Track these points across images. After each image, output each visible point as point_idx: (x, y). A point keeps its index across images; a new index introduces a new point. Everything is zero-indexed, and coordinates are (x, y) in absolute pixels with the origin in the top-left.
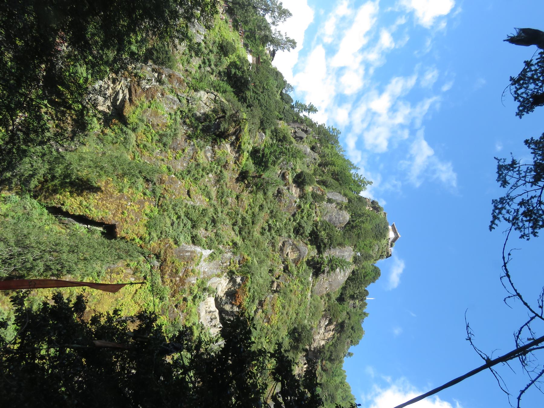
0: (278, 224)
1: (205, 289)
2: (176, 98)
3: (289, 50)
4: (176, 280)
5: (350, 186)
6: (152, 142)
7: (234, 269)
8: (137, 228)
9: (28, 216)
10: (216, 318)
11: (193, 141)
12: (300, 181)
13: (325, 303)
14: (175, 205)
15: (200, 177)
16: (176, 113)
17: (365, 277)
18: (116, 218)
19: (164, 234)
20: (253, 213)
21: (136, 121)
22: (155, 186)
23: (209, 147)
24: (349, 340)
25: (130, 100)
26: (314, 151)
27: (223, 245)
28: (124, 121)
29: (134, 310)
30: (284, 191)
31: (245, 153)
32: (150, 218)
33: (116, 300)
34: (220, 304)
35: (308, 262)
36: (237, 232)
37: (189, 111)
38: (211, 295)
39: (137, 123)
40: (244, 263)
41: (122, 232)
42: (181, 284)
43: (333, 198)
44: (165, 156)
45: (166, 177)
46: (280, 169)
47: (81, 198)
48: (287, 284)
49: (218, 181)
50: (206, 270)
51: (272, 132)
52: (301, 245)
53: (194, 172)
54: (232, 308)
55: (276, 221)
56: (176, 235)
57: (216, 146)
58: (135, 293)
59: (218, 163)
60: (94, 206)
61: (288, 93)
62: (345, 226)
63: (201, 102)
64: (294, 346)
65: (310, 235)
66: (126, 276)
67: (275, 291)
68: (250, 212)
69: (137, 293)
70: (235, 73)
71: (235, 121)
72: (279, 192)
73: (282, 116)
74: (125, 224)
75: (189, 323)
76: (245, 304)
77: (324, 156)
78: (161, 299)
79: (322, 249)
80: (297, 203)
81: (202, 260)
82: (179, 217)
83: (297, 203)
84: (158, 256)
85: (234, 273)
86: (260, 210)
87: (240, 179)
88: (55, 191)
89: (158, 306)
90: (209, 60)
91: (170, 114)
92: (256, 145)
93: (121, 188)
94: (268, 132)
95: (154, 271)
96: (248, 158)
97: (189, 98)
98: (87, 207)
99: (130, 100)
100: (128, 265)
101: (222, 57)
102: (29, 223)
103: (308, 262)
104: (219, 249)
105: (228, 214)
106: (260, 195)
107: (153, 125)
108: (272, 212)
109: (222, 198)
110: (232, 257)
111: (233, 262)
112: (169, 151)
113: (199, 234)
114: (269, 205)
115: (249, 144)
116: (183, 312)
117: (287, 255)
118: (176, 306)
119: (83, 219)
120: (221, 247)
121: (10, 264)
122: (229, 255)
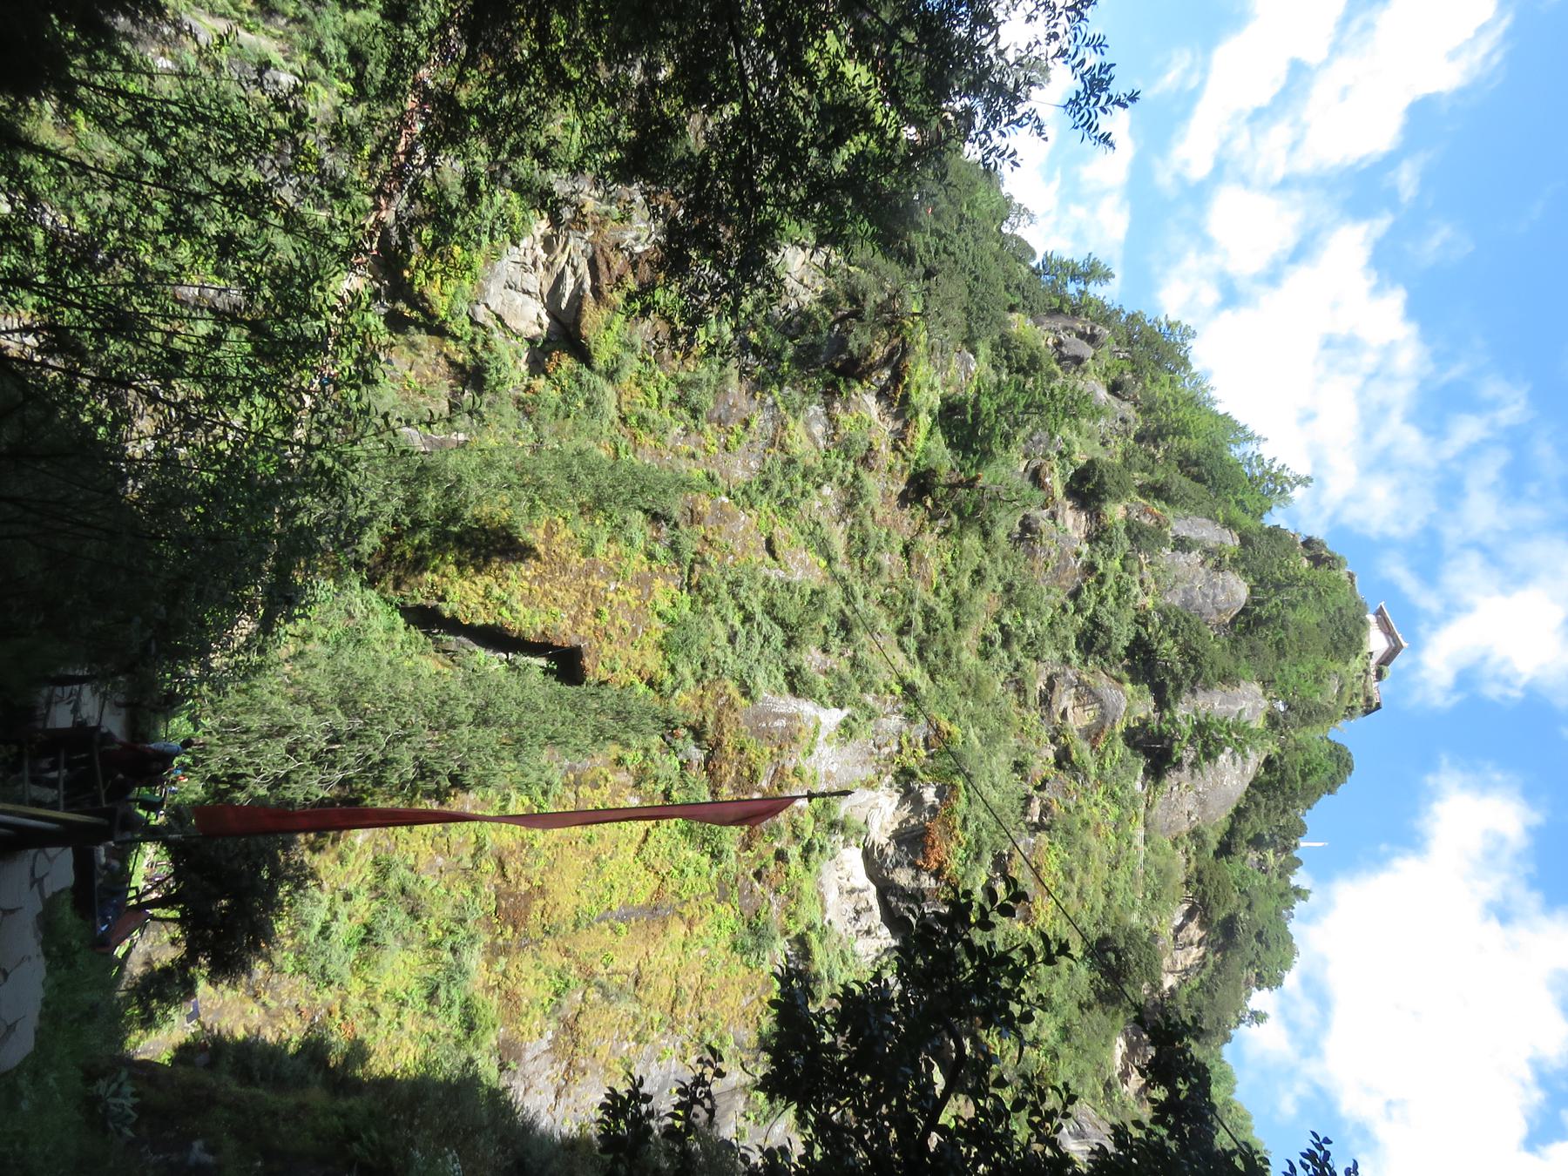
0: (1028, 623)
1: (833, 825)
5: (1239, 497)
6: (660, 407)
7: (912, 763)
8: (637, 653)
10: (871, 909)
11: (770, 394)
12: (1087, 489)
13: (1188, 861)
14: (737, 583)
15: (798, 497)
17: (1304, 776)
18: (582, 630)
19: (711, 667)
20: (955, 594)
21: (616, 349)
22: (677, 533)
23: (820, 410)
24: (1251, 974)
26: (1118, 396)
27: (877, 692)
30: (1042, 524)
32: (672, 623)
33: (596, 860)
34: (881, 868)
35: (1130, 737)
36: (913, 655)
38: (853, 841)
39: (617, 357)
40: (939, 742)
41: (600, 666)
43: (1193, 536)
44: (698, 445)
45: (704, 505)
46: (1026, 456)
47: (487, 579)
48: (1072, 805)
49: (850, 505)
51: (994, 347)
52: (1103, 684)
53: (780, 483)
54: (916, 878)
55: (1023, 615)
57: (837, 405)
58: (645, 840)
59: (847, 451)
60: (517, 598)
61: (1018, 232)
62: (1233, 621)
64: (1107, 992)
65: (1130, 652)
66: (616, 793)
67: (1038, 827)
68: (945, 591)
69: (650, 839)
71: (888, 325)
72: (1027, 526)
73: (1017, 299)
75: (796, 923)
76: (953, 865)
77: (1150, 410)
78: (716, 856)
79: (1169, 695)
80: (1084, 557)
81: (820, 738)
82: (748, 618)
83: (1084, 557)
84: (698, 733)
85: (913, 775)
86: (973, 584)
87: (911, 496)
88: (419, 565)
89: (709, 876)
92: (951, 390)
93: (587, 542)
94: (984, 349)
95: (691, 775)
96: (931, 432)
99: (596, 291)
100: (620, 761)
102: (362, 654)
103: (1130, 737)
104: (865, 706)
106: (972, 541)
108: (1009, 588)
109: (864, 554)
110: (905, 728)
111: (909, 741)
112: (707, 427)
113: (806, 665)
114: (1001, 568)
115: (932, 388)
116: (777, 891)
117: (1064, 715)
118: (758, 875)
119: (495, 638)
120: (869, 698)
122: (895, 721)
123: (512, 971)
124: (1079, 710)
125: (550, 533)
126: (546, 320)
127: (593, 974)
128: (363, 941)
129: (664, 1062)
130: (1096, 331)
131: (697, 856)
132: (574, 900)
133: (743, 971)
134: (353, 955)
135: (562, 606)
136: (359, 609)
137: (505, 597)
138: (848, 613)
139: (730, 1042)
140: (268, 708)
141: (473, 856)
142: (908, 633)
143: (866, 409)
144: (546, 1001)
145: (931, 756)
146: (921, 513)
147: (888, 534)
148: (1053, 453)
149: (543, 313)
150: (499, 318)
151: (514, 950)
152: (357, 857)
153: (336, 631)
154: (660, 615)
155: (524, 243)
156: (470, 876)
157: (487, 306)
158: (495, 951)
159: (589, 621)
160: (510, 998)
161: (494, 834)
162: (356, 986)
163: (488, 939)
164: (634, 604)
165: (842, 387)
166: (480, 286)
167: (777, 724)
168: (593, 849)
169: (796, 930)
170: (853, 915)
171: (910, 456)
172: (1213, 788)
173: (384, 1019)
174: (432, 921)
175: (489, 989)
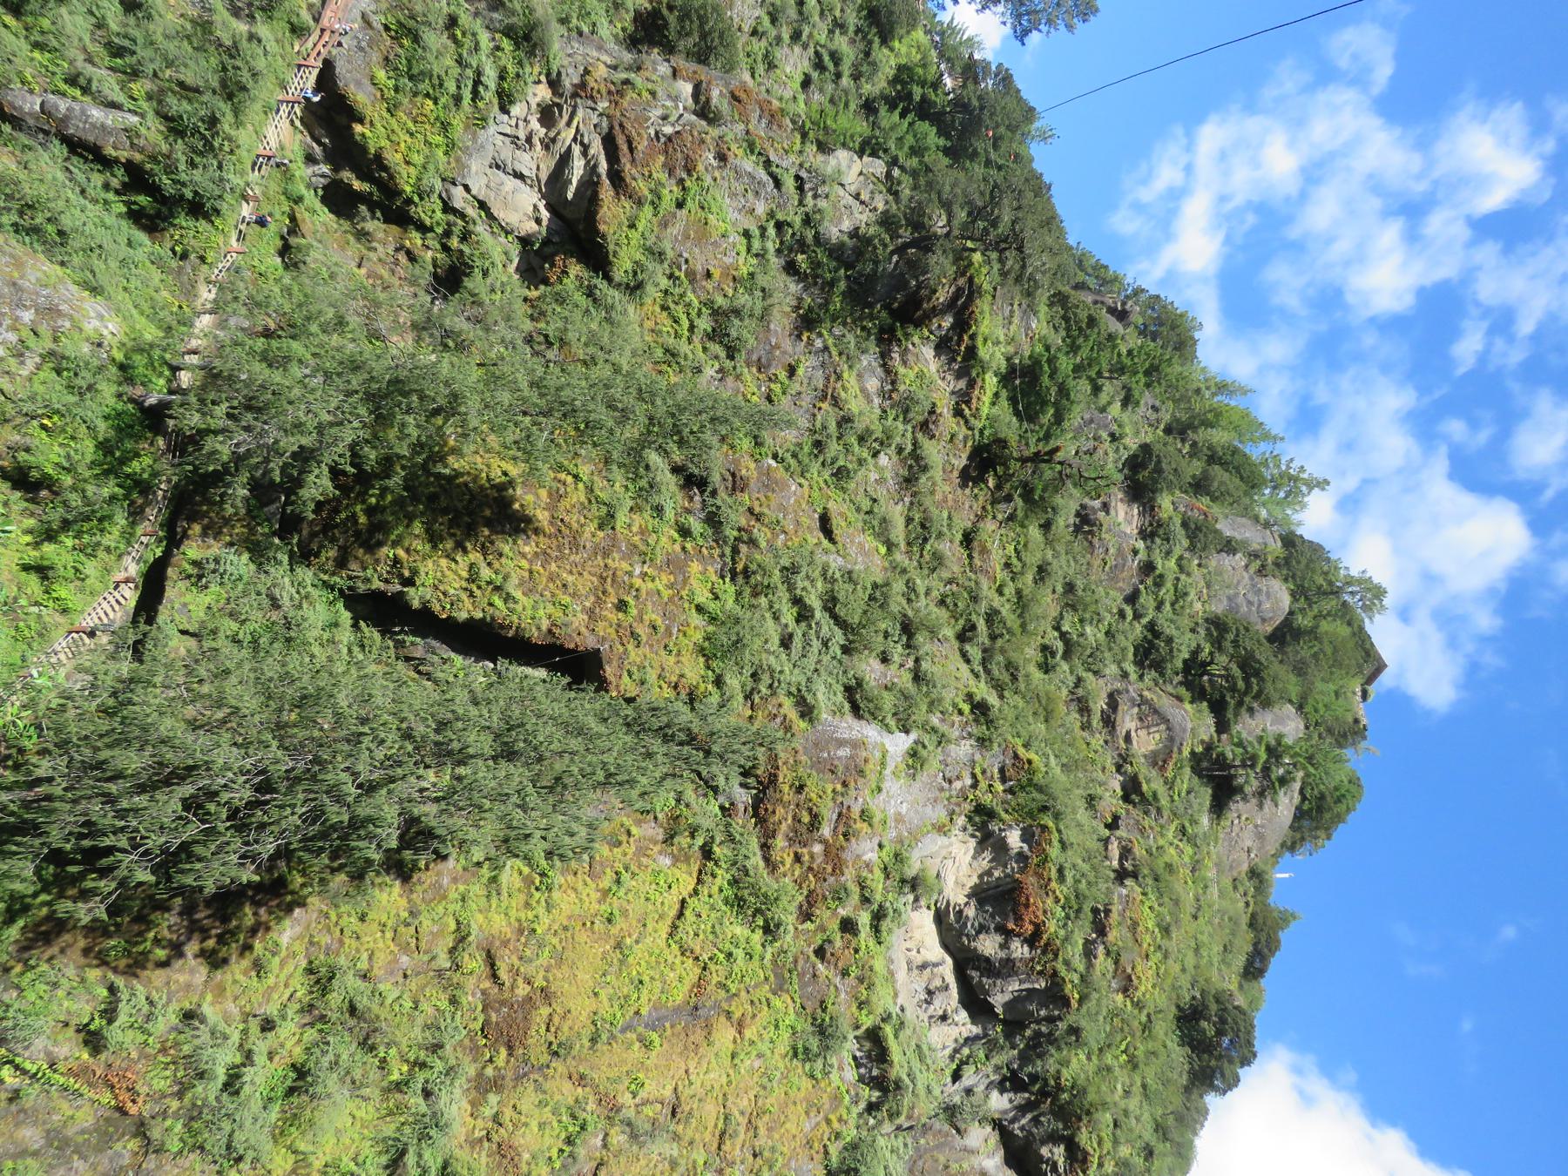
0: (1088, 629)
2: (762, 174)
3: (1070, 27)
4: (812, 856)
7: (987, 799)
8: (672, 659)
9: (288, 634)
10: (947, 988)
11: (820, 335)
13: (1247, 904)
16: (763, 229)
19: (766, 678)
20: (1019, 593)
23: (869, 360)
25: (617, 178)
28: (597, 258)
29: (680, 979)
31: (987, 377)
32: (713, 619)
33: (618, 946)
34: (960, 934)
37: (807, 221)
38: (923, 903)
40: (1019, 777)
42: (829, 869)
43: (1238, 537)
45: (748, 468)
49: (909, 481)
50: (904, 809)
58: (680, 915)
63: (841, 192)
67: (1121, 875)
68: (1009, 590)
69: (688, 913)
70: (923, 96)
74: (630, 647)
78: (770, 930)
79: (1230, 715)
81: (888, 772)
82: (804, 615)
83: (1142, 556)
88: (370, 539)
90: (836, 57)
91: (747, 234)
96: (996, 395)
97: (804, 174)
98: (497, 589)
101: (876, 45)
105: (942, 602)
107: (691, 275)
109: (925, 540)
110: (978, 757)
111: (984, 772)
116: (845, 973)
117: (1128, 738)
119: (484, 640)
120: (935, 720)
121: (262, 826)
122: (963, 750)
123: (508, 1113)
124: (1142, 733)
125: (557, 496)
126: (545, 215)
127: (617, 1109)
128: (291, 1091)
130: (1128, 307)
131: (747, 932)
132: (590, 1004)
133: (806, 1084)
134: (274, 1114)
135: (574, 595)
137: (499, 580)
138: (910, 613)
140: (153, 737)
141: (452, 951)
142: (970, 640)
143: (923, 362)
145: (1010, 791)
146: (983, 495)
147: (950, 518)
148: (1104, 435)
149: (541, 205)
150: (483, 205)
151: (509, 1083)
152: (283, 964)
155: (517, 110)
157: (467, 188)
158: (483, 1086)
159: (614, 616)
161: (480, 918)
163: (471, 1070)
164: (666, 593)
165: (899, 334)
166: (458, 160)
167: (841, 753)
169: (867, 1022)
170: (923, 996)
171: (972, 420)
172: (1270, 820)
174: (393, 1052)
175: (474, 1143)
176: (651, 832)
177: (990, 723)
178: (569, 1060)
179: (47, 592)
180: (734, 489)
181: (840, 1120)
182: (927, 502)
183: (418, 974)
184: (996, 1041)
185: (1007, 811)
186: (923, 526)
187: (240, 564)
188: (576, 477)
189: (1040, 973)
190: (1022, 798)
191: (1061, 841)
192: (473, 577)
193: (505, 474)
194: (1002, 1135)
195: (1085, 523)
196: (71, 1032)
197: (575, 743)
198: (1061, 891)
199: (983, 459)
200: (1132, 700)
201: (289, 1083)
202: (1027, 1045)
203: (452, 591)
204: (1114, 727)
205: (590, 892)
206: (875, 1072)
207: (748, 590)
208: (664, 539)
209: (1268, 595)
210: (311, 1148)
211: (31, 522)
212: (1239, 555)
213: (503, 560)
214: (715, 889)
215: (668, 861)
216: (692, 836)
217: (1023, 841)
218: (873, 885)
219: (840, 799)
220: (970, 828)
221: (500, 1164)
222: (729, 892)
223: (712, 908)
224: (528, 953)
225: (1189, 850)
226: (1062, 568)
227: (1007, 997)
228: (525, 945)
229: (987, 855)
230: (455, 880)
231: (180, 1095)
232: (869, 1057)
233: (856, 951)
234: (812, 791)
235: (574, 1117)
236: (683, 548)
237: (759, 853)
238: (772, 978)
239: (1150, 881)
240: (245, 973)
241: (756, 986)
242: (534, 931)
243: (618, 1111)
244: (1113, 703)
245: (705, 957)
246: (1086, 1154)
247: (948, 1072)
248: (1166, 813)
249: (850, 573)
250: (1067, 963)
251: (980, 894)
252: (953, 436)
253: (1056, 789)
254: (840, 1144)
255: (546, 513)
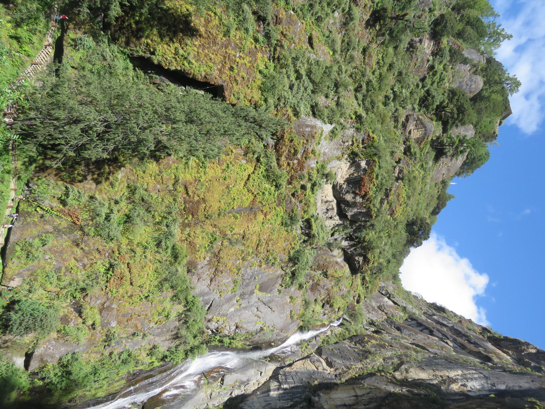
0: (404, 91)
4: (293, 164)
7: (356, 150)
8: (249, 91)
9: (110, 70)
10: (333, 209)
13: (438, 192)
18: (224, 76)
19: (283, 101)
20: (380, 74)
29: (247, 199)
32: (265, 76)
33: (228, 187)
34: (340, 193)
36: (361, 103)
38: (329, 182)
40: (369, 143)
42: (299, 169)
43: (470, 57)
45: (283, 15)
49: (345, 24)
50: (327, 152)
54: (353, 198)
56: (296, 102)
58: (248, 179)
67: (398, 179)
68: (377, 73)
69: (251, 179)
74: (234, 85)
78: (277, 187)
79: (449, 127)
81: (323, 137)
83: (430, 63)
88: (138, 34)
98: (185, 58)
105: (351, 76)
109: (348, 50)
110: (355, 135)
111: (356, 140)
116: (301, 202)
117: (410, 132)
118: (293, 195)
119: (181, 78)
120: (342, 121)
121: (108, 140)
123: (192, 234)
125: (208, 21)
128: (125, 222)
129: (253, 268)
131: (270, 187)
132: (218, 204)
135: (214, 63)
136: (108, 55)
137: (186, 55)
138: (338, 79)
139: (279, 261)
141: (174, 185)
142: (359, 91)
144: (207, 245)
145: (365, 148)
146: (373, 32)
147: (359, 41)
151: (192, 225)
152: (119, 184)
153: (97, 67)
154: (260, 72)
156: (173, 193)
158: (184, 226)
159: (228, 72)
160: (191, 244)
161: (182, 175)
162: (124, 240)
163: (181, 221)
167: (307, 129)
168: (226, 182)
169: (306, 217)
173: (138, 254)
174: (156, 213)
176: (239, 152)
177: (361, 123)
178: (211, 220)
179: (21, 47)
180: (276, 23)
181: (295, 244)
182: (351, 34)
183: (163, 191)
184: (347, 226)
185: (362, 154)
186: (348, 44)
187: (89, 41)
188: (215, 13)
189: (364, 207)
190: (368, 150)
191: (379, 166)
192: (177, 53)
193: (188, 10)
194: (344, 253)
195: (412, 46)
196: (56, 199)
197: (214, 119)
198: (376, 182)
199: (376, 17)
200: (415, 119)
201: (125, 219)
202: (356, 228)
203: (169, 58)
204: (406, 128)
205: (219, 170)
206: (307, 232)
207: (279, 66)
208: (248, 43)
209: (475, 82)
210: (133, 238)
211: (9, 18)
212: (468, 65)
213: (188, 47)
214: (260, 172)
215: (245, 162)
216: (253, 154)
217: (366, 165)
218: (313, 175)
219: (305, 145)
220: (349, 159)
221: (190, 247)
222: (264, 173)
223: (259, 178)
224: (198, 187)
225: (423, 173)
226: (399, 65)
227: (352, 213)
228: (197, 185)
229: (353, 168)
230: (174, 162)
231: (92, 220)
232: (305, 227)
233: (305, 195)
234: (296, 142)
235: (212, 236)
236: (256, 47)
237: (276, 161)
238: (277, 201)
239: (407, 181)
240: (108, 186)
241: (271, 203)
242: (200, 180)
243: (226, 235)
244: (407, 119)
245: (256, 193)
246: (369, 260)
247: (330, 234)
248: (418, 160)
249: (318, 61)
250: (374, 205)
251: (349, 181)
252: (366, 5)
253: (381, 148)
254: (294, 251)
255: (204, 28)
